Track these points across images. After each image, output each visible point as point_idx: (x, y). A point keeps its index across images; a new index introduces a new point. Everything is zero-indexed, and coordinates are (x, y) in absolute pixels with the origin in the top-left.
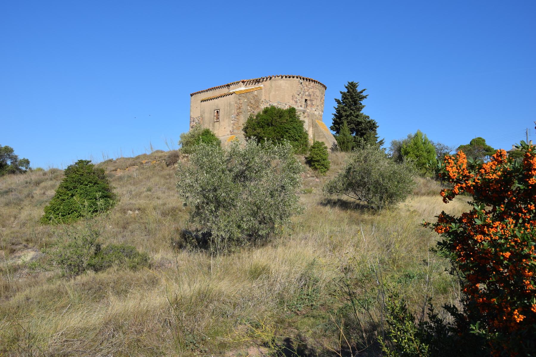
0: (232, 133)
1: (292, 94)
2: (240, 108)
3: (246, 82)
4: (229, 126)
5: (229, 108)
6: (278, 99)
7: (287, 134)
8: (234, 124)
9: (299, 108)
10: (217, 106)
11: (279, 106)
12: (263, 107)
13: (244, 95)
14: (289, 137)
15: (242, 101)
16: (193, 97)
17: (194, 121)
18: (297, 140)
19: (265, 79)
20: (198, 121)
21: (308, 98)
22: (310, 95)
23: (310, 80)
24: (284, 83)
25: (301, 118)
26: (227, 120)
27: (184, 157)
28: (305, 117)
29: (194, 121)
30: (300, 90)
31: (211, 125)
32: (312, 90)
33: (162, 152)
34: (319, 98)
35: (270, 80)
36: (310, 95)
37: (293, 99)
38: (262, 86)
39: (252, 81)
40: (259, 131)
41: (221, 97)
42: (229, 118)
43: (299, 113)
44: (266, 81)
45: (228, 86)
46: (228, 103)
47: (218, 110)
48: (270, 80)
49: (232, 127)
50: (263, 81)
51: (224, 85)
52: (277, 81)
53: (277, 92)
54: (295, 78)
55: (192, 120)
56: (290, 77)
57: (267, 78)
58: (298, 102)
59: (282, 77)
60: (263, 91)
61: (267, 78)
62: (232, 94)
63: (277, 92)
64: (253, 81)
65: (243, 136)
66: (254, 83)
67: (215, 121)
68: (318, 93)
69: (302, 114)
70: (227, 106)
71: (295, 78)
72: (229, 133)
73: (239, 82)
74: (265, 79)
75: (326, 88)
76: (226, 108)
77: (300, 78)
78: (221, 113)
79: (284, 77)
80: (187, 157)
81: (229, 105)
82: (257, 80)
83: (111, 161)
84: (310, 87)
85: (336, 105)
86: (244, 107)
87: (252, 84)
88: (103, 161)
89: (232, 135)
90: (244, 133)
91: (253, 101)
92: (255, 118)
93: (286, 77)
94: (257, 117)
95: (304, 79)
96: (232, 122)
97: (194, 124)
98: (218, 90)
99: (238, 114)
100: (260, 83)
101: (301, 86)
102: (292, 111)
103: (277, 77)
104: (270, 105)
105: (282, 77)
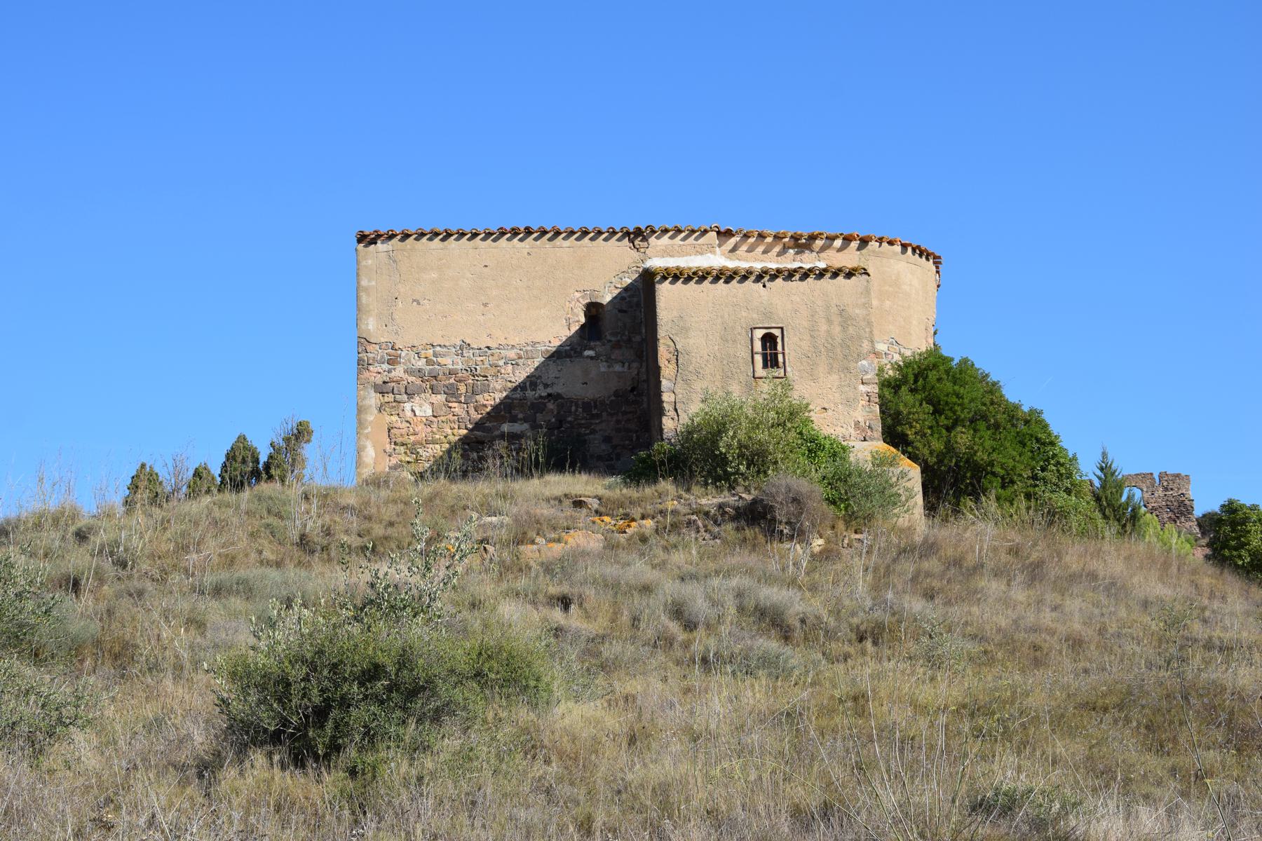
3: (733, 241)
4: (849, 403)
5: (837, 329)
6: (890, 327)
10: (768, 314)
16: (380, 246)
17: (393, 361)
20: (429, 362)
26: (835, 377)
35: (859, 249)
39: (769, 240)
44: (839, 250)
45: (637, 235)
46: (834, 310)
47: (777, 332)
48: (859, 249)
50: (823, 249)
52: (885, 260)
53: (888, 303)
59: (904, 246)
62: (849, 275)
63: (888, 303)
64: (777, 237)
66: (777, 249)
70: (829, 321)
73: (706, 232)
74: (838, 243)
76: (823, 327)
78: (791, 349)
79: (910, 249)
81: (837, 320)
82: (795, 238)
87: (765, 252)
93: (914, 250)
96: (863, 388)
97: (399, 372)
98: (567, 243)
103: (885, 244)
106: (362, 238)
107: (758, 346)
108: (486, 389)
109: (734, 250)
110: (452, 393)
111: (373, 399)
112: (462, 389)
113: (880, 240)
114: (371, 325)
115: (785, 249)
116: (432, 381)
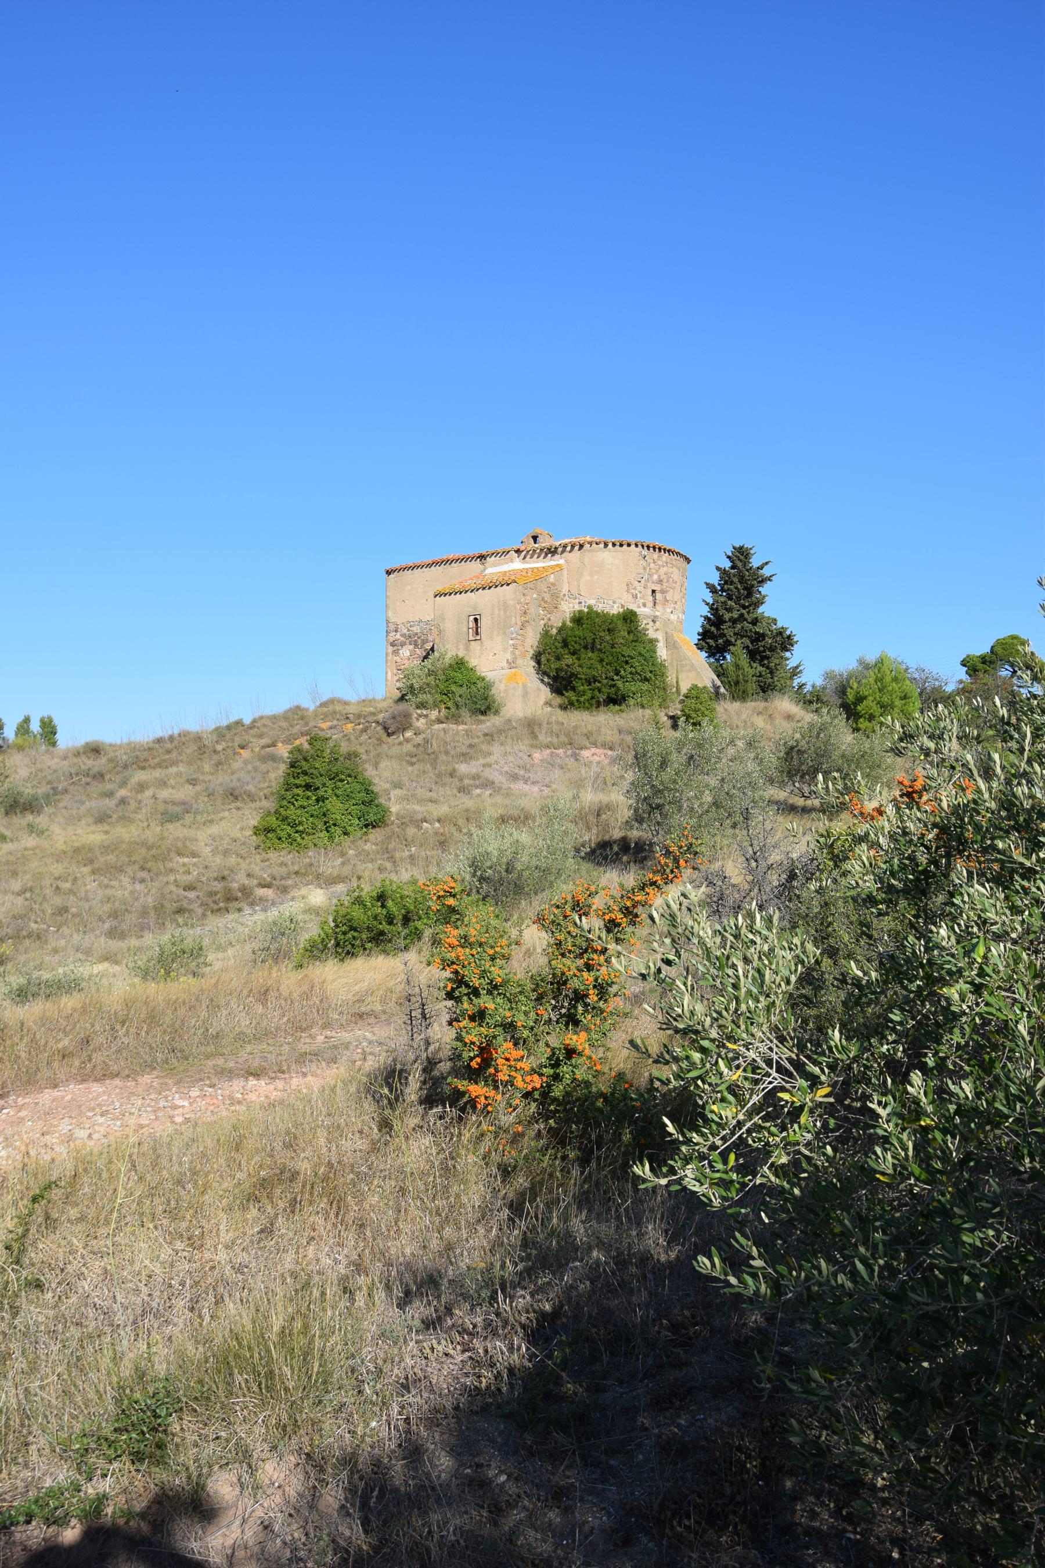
0: (512, 664)
1: (626, 580)
2: (525, 613)
5: (502, 613)
7: (627, 667)
8: (515, 647)
9: (643, 611)
11: (600, 608)
12: (568, 608)
13: (532, 586)
14: (631, 673)
15: (528, 598)
16: (392, 576)
17: (396, 631)
18: (647, 680)
19: (569, 548)
21: (657, 587)
22: (660, 581)
23: (660, 549)
24: (608, 556)
25: (651, 634)
27: (420, 716)
28: (657, 630)
29: (396, 631)
30: (642, 571)
31: (461, 646)
32: (665, 569)
33: (346, 703)
34: (678, 586)
36: (660, 581)
37: (628, 591)
38: (562, 562)
40: (570, 662)
41: (484, 589)
42: (504, 633)
43: (645, 622)
44: (570, 552)
45: (482, 557)
49: (513, 653)
50: (563, 552)
51: (471, 554)
54: (633, 546)
55: (392, 627)
56: (621, 545)
57: (573, 547)
58: (639, 595)
59: (606, 545)
60: (565, 572)
61: (573, 547)
64: (541, 550)
65: (533, 671)
67: (471, 638)
68: (676, 575)
69: (651, 624)
70: (499, 609)
71: (633, 546)
72: (505, 664)
74: (569, 548)
75: (688, 560)
76: (497, 612)
77: (643, 546)
78: (484, 624)
79: (610, 545)
80: (426, 716)
82: (549, 549)
83: (239, 723)
84: (660, 563)
85: (709, 598)
86: (533, 611)
88: (225, 723)
89: (513, 670)
90: (534, 664)
91: (547, 597)
92: (554, 631)
93: (614, 545)
94: (560, 630)
95: (648, 547)
96: (511, 642)
97: (398, 636)
99: (523, 627)
100: (557, 556)
101: (644, 563)
102: (629, 618)
103: (594, 545)
104: (580, 603)
105: (606, 545)
106: (388, 573)
107: (472, 624)
108: (427, 641)
109: (524, 558)
110: (416, 645)
111: (390, 649)
112: (419, 641)
113: (590, 543)
114: (390, 614)
115: (546, 555)
116: (414, 640)
